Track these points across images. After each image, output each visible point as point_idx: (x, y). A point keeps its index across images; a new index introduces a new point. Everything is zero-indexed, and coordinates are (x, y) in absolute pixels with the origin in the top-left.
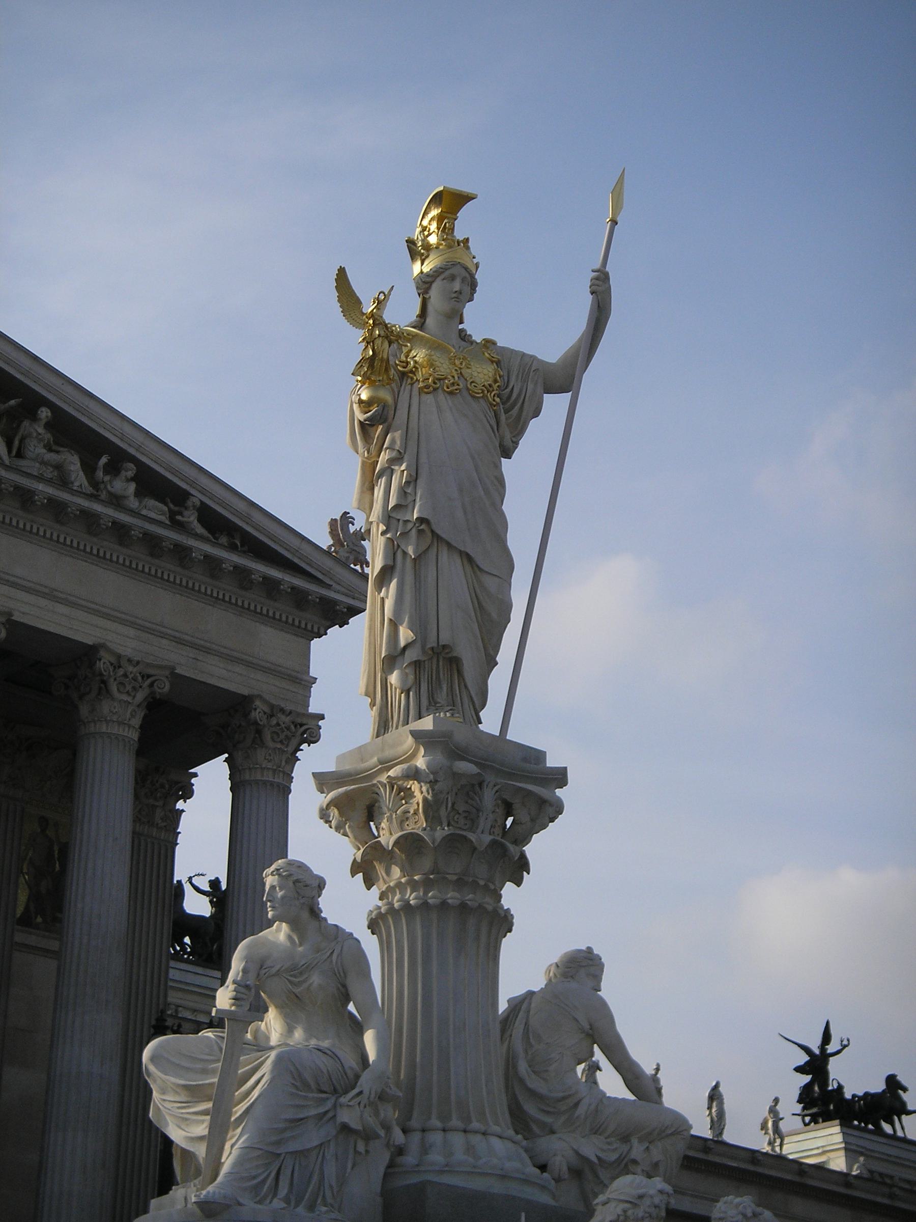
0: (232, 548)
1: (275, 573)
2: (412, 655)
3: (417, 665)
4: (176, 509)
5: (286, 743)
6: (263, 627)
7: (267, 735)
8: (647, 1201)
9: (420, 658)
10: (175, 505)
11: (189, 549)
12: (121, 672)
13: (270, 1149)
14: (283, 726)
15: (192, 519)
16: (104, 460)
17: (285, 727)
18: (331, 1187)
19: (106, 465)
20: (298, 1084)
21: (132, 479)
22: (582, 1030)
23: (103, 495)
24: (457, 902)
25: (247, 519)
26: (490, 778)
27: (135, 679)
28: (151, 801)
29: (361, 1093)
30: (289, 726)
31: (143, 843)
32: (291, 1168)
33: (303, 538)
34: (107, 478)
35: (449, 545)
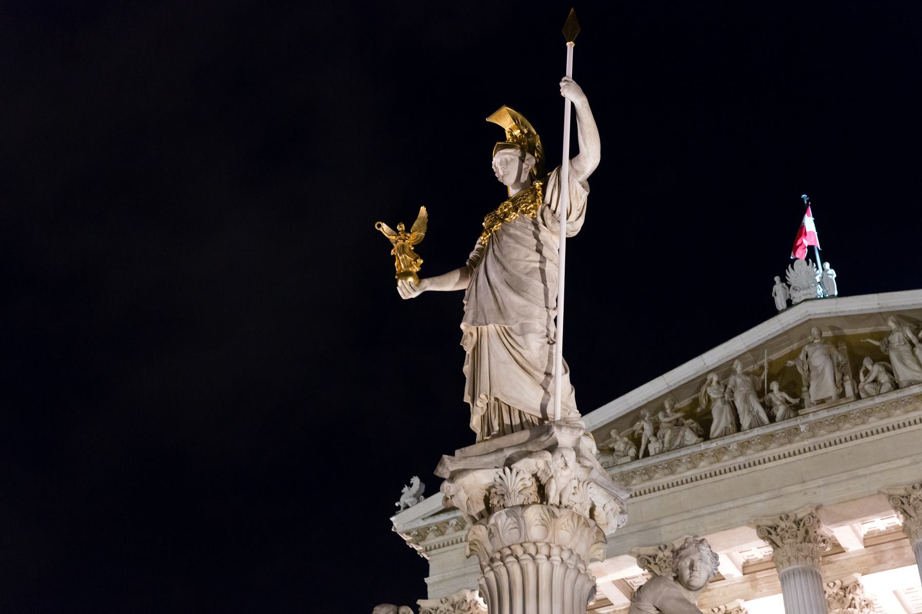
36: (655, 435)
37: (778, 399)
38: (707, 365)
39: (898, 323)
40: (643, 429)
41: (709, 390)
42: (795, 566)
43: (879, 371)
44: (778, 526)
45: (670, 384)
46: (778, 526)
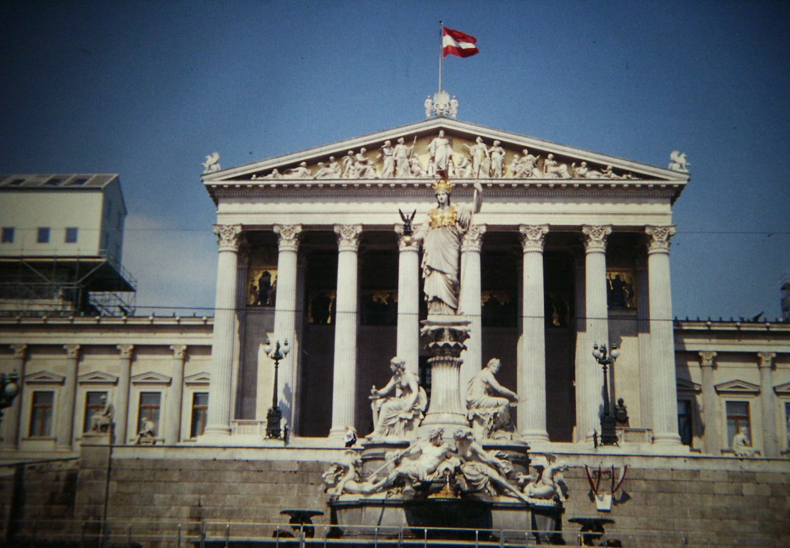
0: (628, 179)
1: (645, 182)
3: (431, 302)
12: (593, 231)
21: (587, 166)
22: (484, 382)
23: (577, 177)
26: (446, 327)
35: (437, 271)
39: (481, 142)
40: (347, 162)
41: (384, 149)
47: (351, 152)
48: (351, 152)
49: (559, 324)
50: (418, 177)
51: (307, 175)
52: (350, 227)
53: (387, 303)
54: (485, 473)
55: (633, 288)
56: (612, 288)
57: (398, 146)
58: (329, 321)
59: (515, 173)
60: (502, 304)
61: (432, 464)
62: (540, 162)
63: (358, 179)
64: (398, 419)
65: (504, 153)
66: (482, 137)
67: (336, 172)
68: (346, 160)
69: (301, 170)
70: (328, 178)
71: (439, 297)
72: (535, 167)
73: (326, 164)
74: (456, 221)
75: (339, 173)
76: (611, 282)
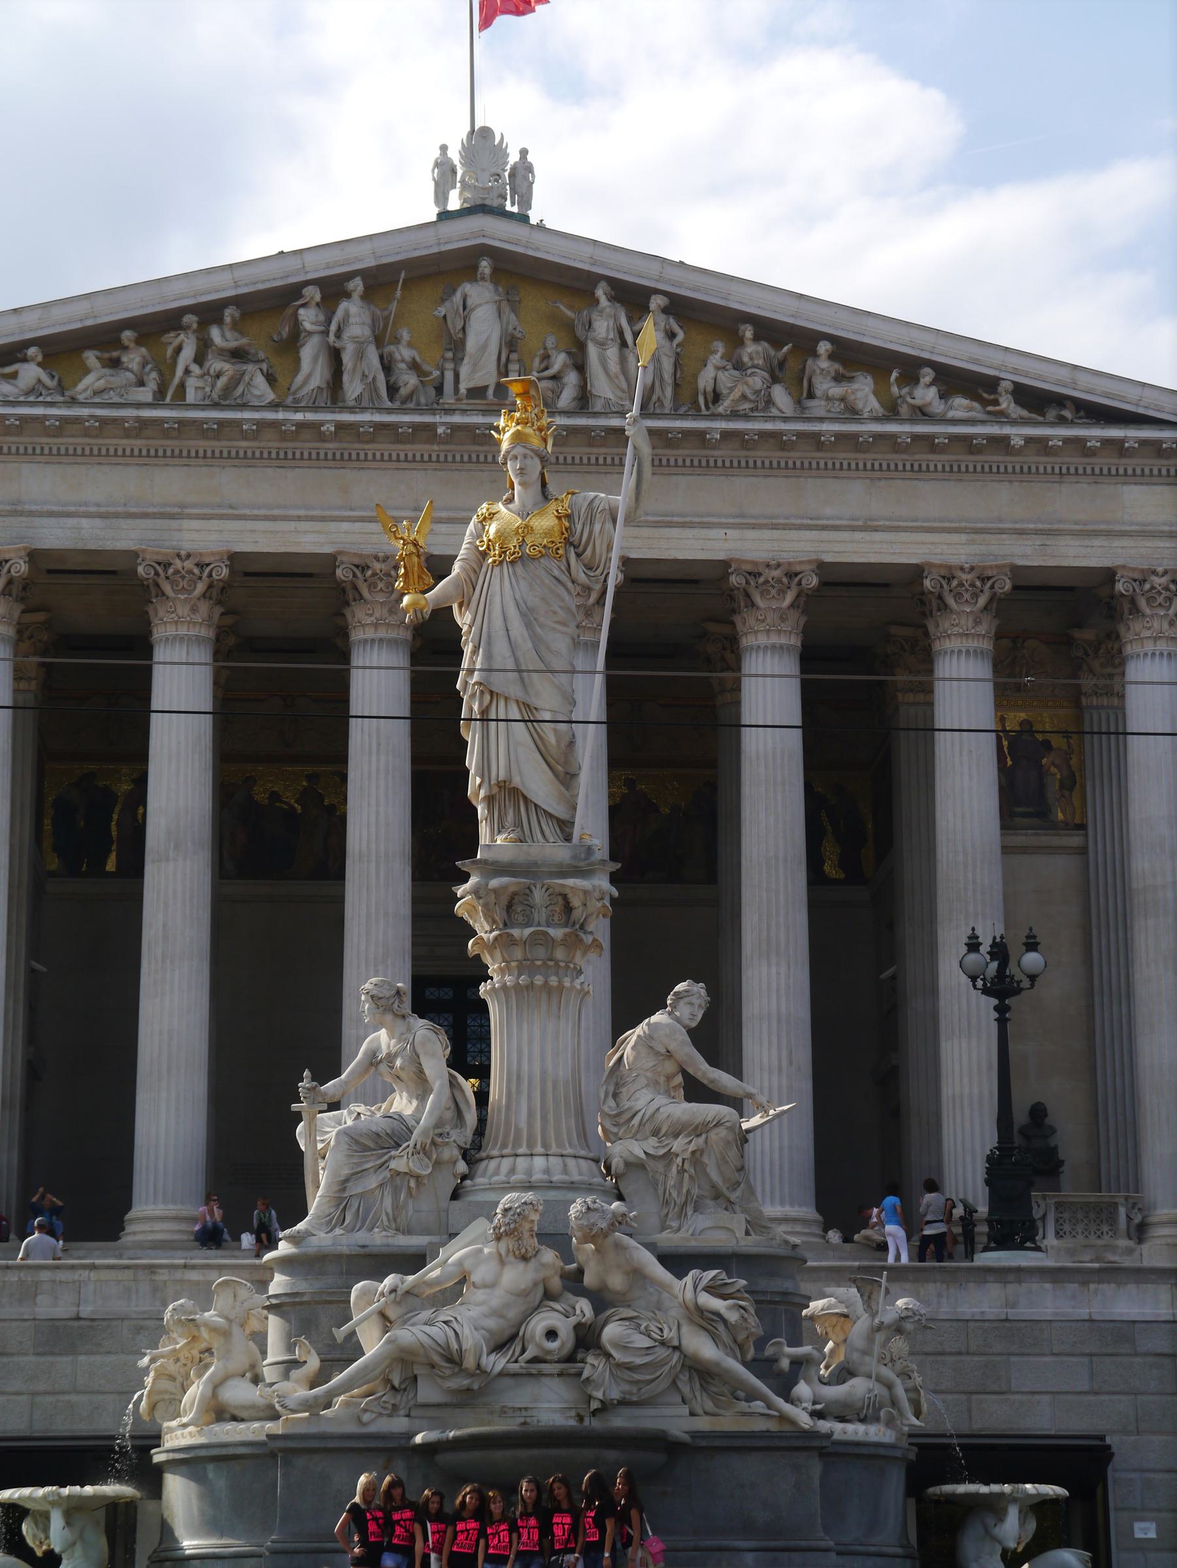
0: (1062, 421)
2: (482, 793)
4: (992, 397)
5: (1168, 604)
6: (1126, 488)
7: (1142, 603)
8: (511, 1213)
9: (488, 794)
10: (990, 393)
11: (1006, 439)
12: (955, 583)
13: (337, 1195)
14: (1159, 588)
15: (1004, 406)
16: (895, 375)
17: (1163, 589)
18: (387, 1214)
19: (897, 379)
20: (354, 1148)
21: (931, 384)
22: (658, 1054)
24: (512, 984)
25: (1074, 385)
27: (973, 585)
28: (1109, 670)
29: (408, 1146)
30: (1168, 585)
31: (1104, 717)
32: (356, 1206)
33: (1144, 385)
34: (905, 391)
36: (199, 359)
37: (403, 361)
38: (307, 269)
39: (611, 299)
40: (179, 349)
41: (302, 311)
42: (382, 633)
43: (565, 366)
44: (368, 567)
45: (239, 283)
46: (368, 567)
47: (190, 319)
48: (190, 319)
49: (842, 876)
50: (411, 405)
51: (48, 389)
52: (189, 564)
53: (298, 808)
54: (676, 1343)
55: (1074, 761)
56: (1010, 763)
57: (344, 305)
58: (111, 865)
59: (717, 397)
60: (666, 810)
61: (502, 1316)
62: (793, 365)
63: (216, 405)
64: (387, 1174)
65: (681, 336)
66: (613, 282)
67: (141, 383)
68: (176, 342)
69: (30, 373)
70: (117, 400)
71: (516, 782)
72: (775, 380)
73: (106, 355)
74: (568, 542)
75: (152, 385)
76: (1005, 743)
